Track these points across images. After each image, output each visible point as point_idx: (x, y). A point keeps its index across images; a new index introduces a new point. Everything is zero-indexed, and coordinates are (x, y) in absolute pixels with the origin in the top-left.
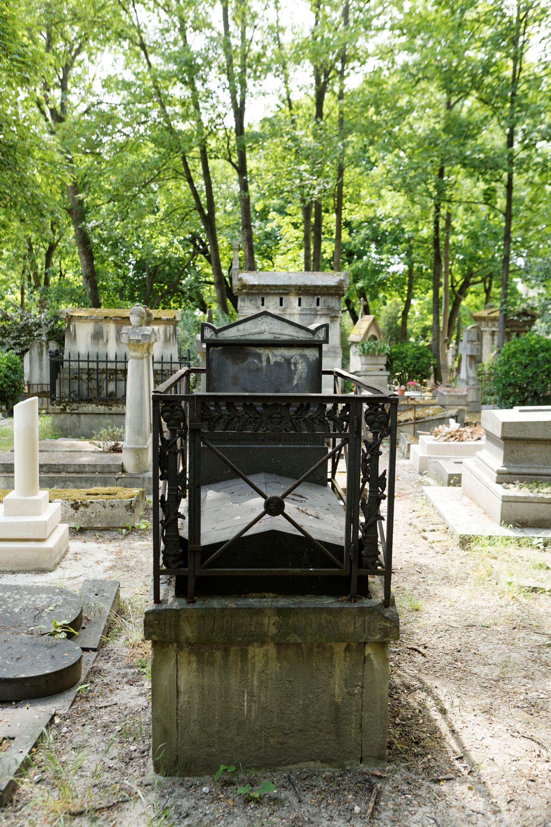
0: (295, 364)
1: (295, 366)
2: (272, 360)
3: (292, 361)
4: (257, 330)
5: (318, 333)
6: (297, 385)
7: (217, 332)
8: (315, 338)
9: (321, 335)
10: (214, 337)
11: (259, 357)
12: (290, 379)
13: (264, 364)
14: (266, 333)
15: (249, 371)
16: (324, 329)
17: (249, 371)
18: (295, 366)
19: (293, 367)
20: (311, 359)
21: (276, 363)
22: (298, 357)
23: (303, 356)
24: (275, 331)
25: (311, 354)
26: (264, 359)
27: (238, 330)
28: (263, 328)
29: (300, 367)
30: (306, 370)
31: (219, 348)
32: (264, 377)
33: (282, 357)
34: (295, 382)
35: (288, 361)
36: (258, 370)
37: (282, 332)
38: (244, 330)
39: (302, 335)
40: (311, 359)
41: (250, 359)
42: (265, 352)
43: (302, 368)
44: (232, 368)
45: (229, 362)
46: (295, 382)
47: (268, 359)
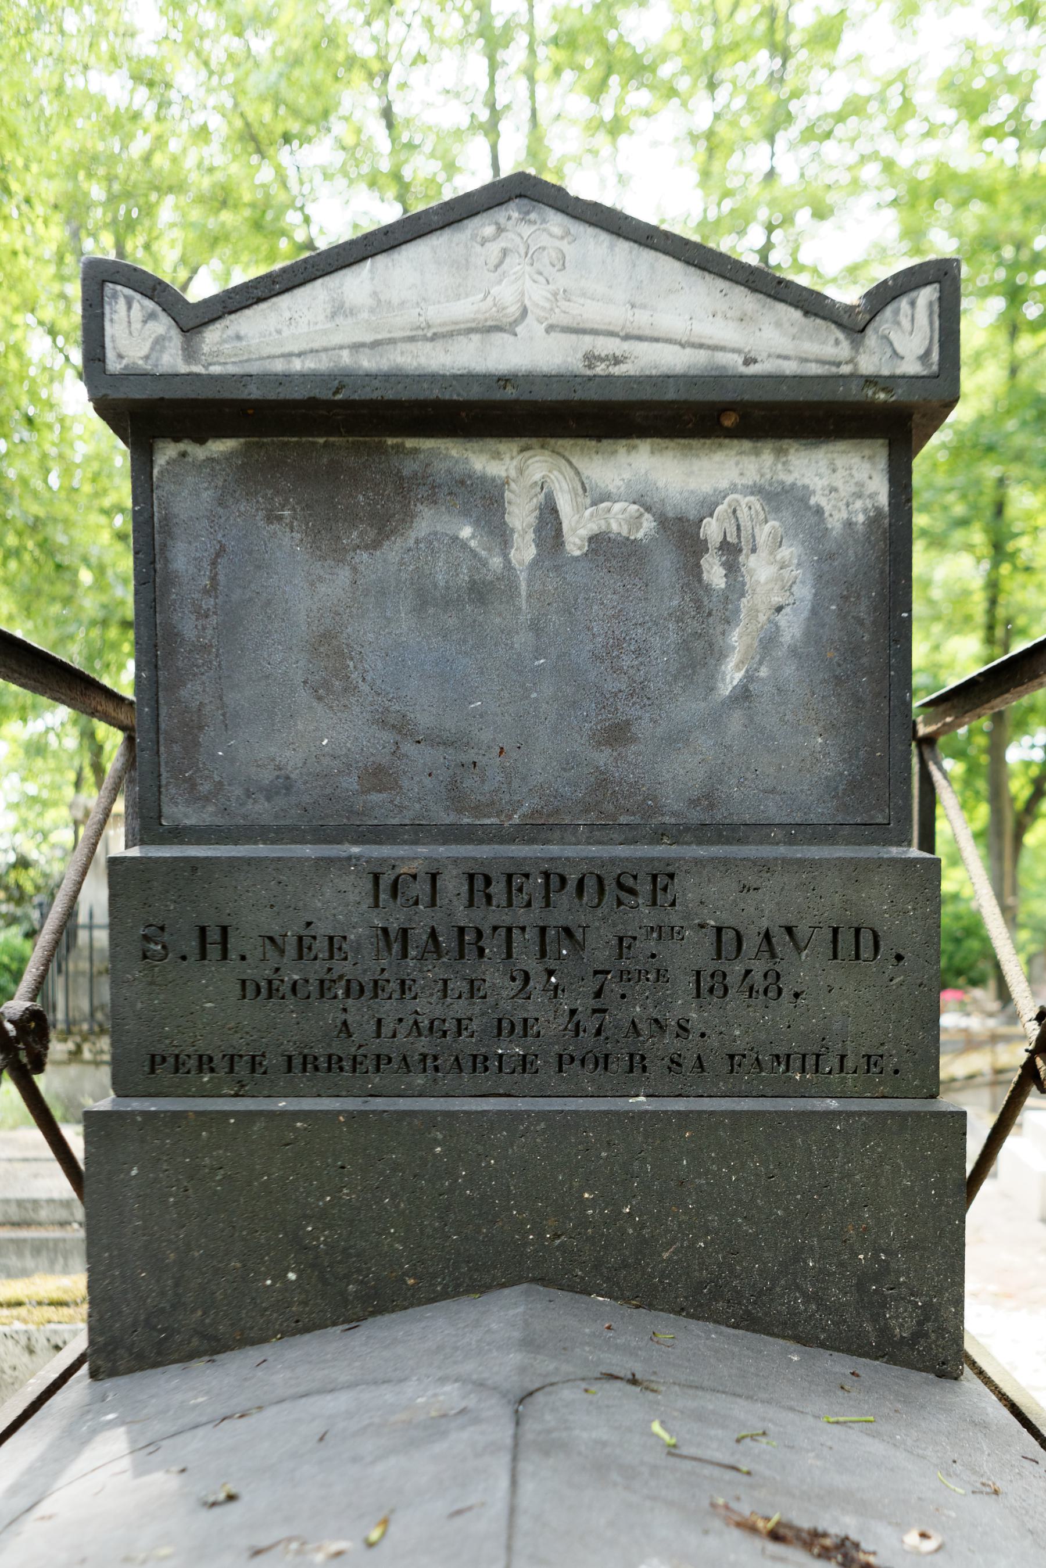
0: (730, 551)
1: (732, 568)
2: (578, 528)
3: (712, 530)
4: (465, 309)
5: (885, 322)
6: (744, 694)
7: (193, 320)
8: (870, 362)
9: (904, 344)
10: (172, 360)
11: (487, 502)
12: (699, 656)
13: (524, 551)
14: (532, 327)
15: (424, 599)
16: (927, 295)
17: (424, 599)
18: (732, 568)
19: (714, 573)
20: (835, 521)
21: (600, 544)
22: (749, 505)
23: (778, 498)
24: (592, 313)
25: (843, 480)
26: (521, 515)
27: (339, 310)
28: (506, 295)
29: (760, 569)
30: (804, 592)
31: (220, 447)
32: (523, 639)
33: (644, 502)
34: (732, 675)
35: (683, 533)
36: (480, 592)
37: (642, 320)
38: (379, 304)
39: (774, 346)
40: (835, 521)
41: (428, 522)
42: (524, 473)
43: (775, 583)
44: (303, 580)
45: (287, 544)
46: (732, 675)
47: (549, 518)
